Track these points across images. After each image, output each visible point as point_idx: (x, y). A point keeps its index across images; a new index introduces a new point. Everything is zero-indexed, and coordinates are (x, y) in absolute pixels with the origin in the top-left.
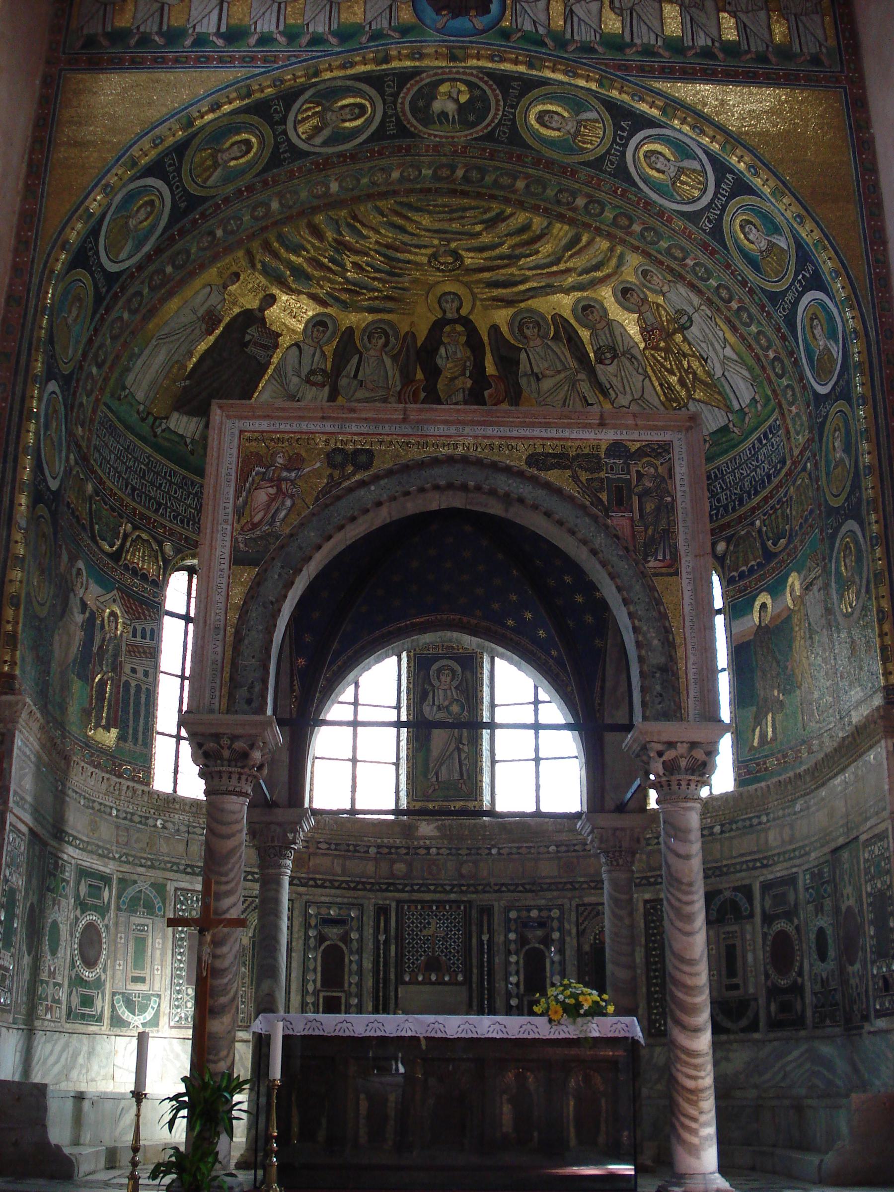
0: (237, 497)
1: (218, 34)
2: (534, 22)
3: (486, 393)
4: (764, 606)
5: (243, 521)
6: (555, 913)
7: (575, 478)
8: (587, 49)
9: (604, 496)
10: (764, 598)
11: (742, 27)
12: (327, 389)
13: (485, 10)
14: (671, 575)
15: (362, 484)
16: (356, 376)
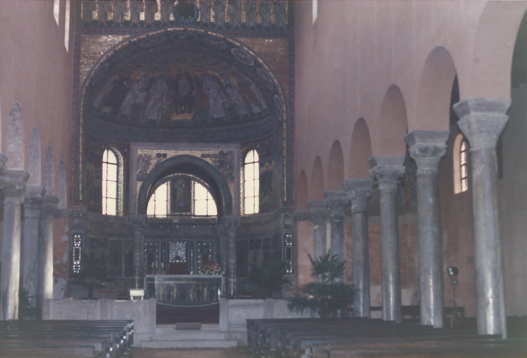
0: (137, 165)
1: (122, 23)
2: (207, 19)
3: (193, 93)
4: (267, 166)
5: (139, 171)
6: (210, 244)
7: (211, 159)
8: (220, 28)
9: (218, 164)
10: (267, 164)
11: (263, 19)
12: (146, 93)
13: (193, 16)
14: (232, 183)
15: (165, 162)
16: (155, 88)
